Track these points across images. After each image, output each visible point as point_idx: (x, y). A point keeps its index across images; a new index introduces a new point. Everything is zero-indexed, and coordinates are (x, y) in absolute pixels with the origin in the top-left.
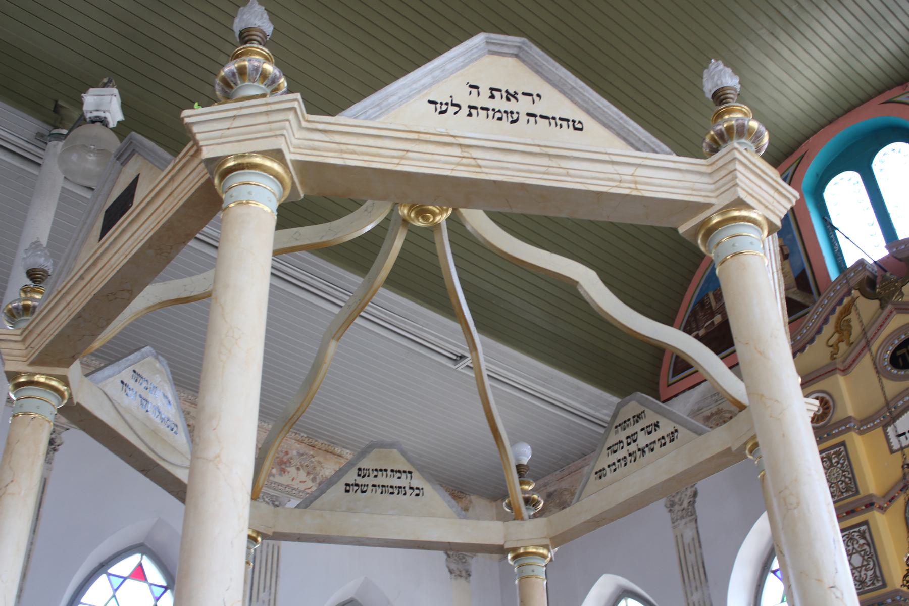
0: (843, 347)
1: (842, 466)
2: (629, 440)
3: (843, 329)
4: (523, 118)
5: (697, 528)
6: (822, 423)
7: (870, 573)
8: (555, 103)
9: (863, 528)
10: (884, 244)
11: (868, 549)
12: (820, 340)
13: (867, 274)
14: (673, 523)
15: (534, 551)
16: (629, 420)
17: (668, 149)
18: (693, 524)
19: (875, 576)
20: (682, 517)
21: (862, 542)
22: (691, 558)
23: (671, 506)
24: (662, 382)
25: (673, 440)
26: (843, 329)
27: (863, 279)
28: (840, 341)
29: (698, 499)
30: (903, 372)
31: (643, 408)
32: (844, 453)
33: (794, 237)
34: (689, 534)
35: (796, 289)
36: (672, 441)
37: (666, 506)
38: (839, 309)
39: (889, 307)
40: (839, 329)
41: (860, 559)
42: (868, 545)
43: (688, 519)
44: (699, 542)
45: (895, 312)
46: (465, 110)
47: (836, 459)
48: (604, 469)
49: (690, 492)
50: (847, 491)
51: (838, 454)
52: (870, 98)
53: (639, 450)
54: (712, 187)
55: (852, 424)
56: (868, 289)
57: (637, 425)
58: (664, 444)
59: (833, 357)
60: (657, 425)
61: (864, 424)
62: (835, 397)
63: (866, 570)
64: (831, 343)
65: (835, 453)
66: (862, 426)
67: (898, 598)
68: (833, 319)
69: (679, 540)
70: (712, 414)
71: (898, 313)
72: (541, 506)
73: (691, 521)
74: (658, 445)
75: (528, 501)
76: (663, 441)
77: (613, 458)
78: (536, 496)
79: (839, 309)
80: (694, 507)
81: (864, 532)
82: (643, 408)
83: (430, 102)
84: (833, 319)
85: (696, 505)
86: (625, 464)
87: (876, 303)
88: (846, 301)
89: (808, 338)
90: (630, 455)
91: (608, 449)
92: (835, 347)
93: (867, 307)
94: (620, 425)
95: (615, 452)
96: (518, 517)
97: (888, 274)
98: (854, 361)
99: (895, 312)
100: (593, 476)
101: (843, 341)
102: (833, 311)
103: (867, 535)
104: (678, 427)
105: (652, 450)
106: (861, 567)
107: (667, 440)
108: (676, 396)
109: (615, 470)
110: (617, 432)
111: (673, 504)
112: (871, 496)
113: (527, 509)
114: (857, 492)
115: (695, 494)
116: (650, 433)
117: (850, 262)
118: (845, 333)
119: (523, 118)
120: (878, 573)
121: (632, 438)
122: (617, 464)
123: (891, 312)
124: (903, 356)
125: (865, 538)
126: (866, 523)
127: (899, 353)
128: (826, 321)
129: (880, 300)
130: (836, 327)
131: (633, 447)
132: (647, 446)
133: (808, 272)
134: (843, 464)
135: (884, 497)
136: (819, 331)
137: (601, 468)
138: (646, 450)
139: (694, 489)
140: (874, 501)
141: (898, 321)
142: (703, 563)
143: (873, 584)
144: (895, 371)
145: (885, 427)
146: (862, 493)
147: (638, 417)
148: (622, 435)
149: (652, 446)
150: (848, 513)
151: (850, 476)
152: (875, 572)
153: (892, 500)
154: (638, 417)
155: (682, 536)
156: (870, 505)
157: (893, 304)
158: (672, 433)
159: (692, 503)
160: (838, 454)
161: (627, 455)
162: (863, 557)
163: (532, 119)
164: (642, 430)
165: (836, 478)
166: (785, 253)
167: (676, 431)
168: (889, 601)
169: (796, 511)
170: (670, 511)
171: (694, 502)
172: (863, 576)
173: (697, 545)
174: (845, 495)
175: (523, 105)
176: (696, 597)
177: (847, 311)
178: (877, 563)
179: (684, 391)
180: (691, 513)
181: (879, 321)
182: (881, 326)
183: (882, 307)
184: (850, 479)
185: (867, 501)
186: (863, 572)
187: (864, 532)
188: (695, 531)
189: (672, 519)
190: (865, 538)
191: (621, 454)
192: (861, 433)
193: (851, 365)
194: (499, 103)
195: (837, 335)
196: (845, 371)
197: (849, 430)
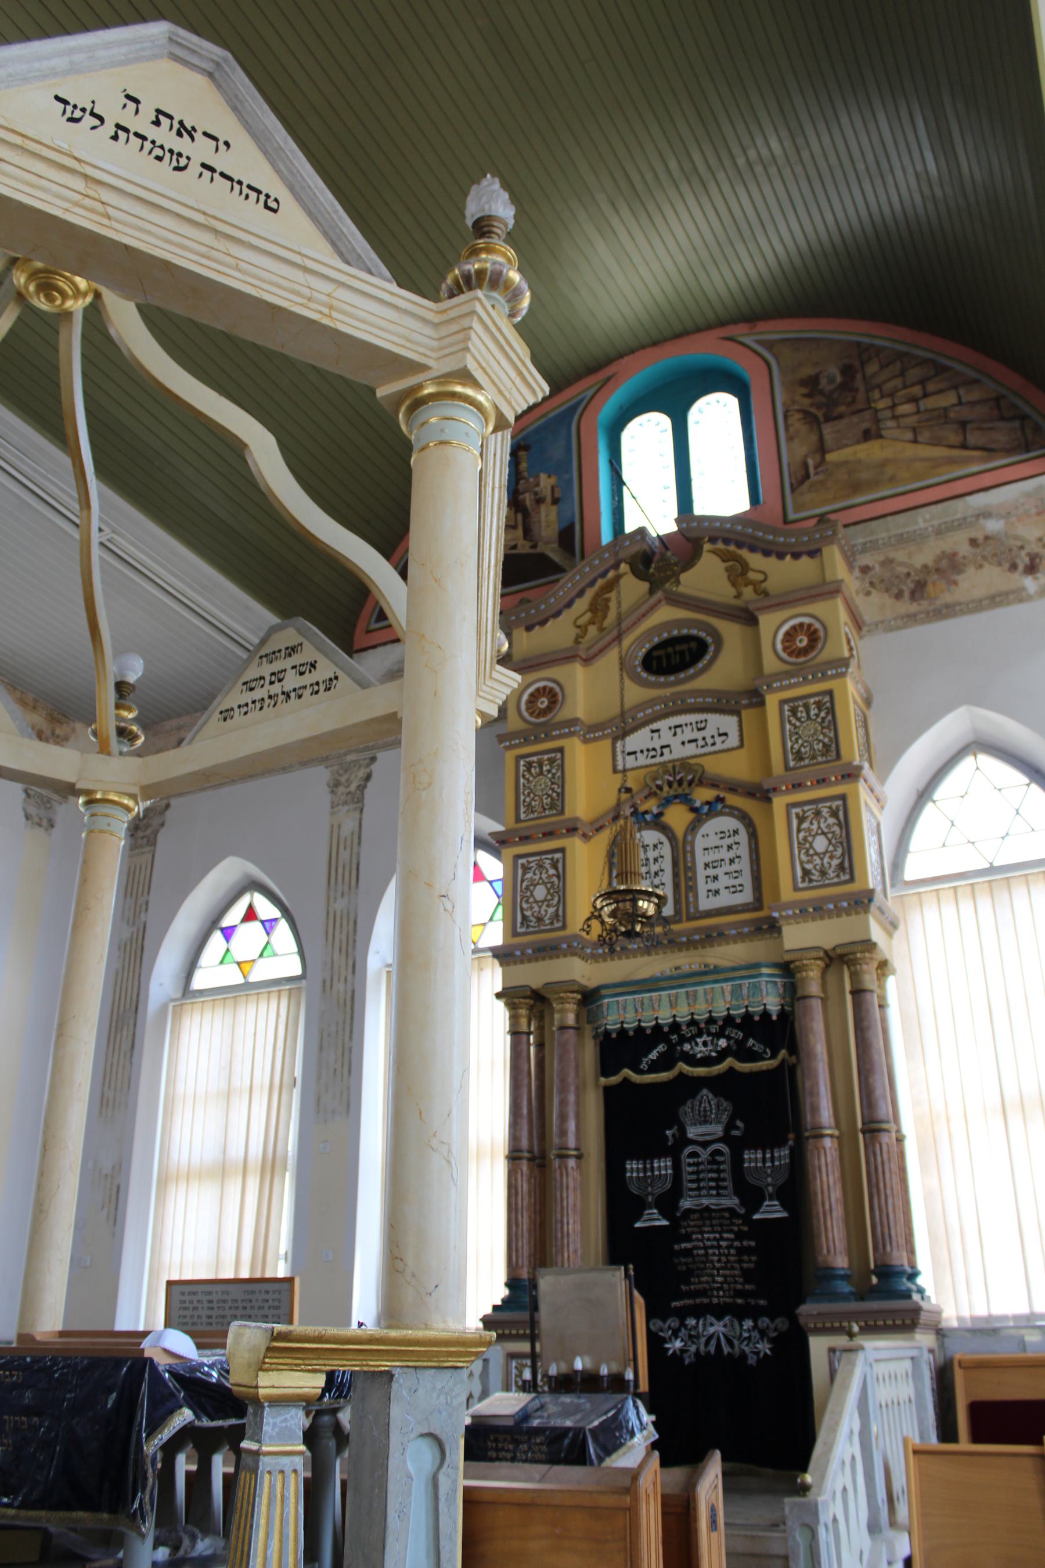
0: (593, 630)
1: (553, 777)
2: (273, 678)
3: (599, 608)
4: (195, 168)
5: (361, 820)
6: (542, 720)
7: (551, 910)
8: (247, 161)
10: (676, 516)
11: (556, 882)
12: (567, 617)
13: (645, 547)
14: (332, 807)
15: (116, 799)
16: (280, 651)
17: (388, 274)
18: (357, 814)
19: (556, 915)
20: (345, 803)
21: (552, 872)
22: (344, 855)
23: (335, 785)
24: (361, 625)
25: (329, 689)
26: (599, 608)
27: (638, 552)
28: (591, 622)
29: (369, 784)
30: (653, 678)
31: (301, 639)
32: (559, 762)
33: (571, 480)
34: (349, 825)
35: (555, 545)
36: (328, 689)
37: (328, 785)
38: (600, 582)
39: (659, 594)
40: (593, 608)
41: (545, 891)
42: (558, 877)
43: (352, 806)
44: (360, 838)
45: (664, 602)
46: (109, 129)
47: (548, 767)
48: (232, 709)
49: (362, 773)
50: (550, 809)
51: (551, 761)
52: (709, 327)
53: (283, 693)
54: (435, 344)
55: (578, 728)
56: (641, 567)
57: (288, 659)
58: (317, 692)
59: (577, 641)
60: (313, 665)
61: (592, 732)
62: (567, 690)
63: (548, 906)
64: (580, 622)
65: (548, 759)
66: (589, 733)
67: (575, 944)
68: (590, 593)
69: (335, 830)
71: (668, 604)
72: (139, 742)
73: (355, 809)
74: (309, 691)
75: (122, 732)
76: (316, 688)
77: (248, 697)
78: (135, 728)
79: (600, 582)
81: (558, 861)
82: (301, 639)
83: (57, 98)
84: (590, 593)
85: (366, 791)
86: (261, 708)
87: (645, 586)
88: (611, 574)
89: (553, 611)
90: (270, 697)
91: (245, 683)
92: (583, 629)
93: (632, 588)
94: (266, 655)
95: (251, 689)
96: (104, 749)
97: (669, 554)
98: (601, 651)
99: (664, 602)
100: (217, 715)
101: (594, 623)
102: (592, 583)
103: (560, 866)
104: (339, 673)
105: (300, 697)
106: (543, 902)
107: (322, 687)
108: (374, 647)
109: (246, 713)
110: (260, 664)
111: (337, 784)
112: (576, 819)
113: (119, 742)
114: (562, 812)
115: (368, 777)
116: (302, 674)
117: (629, 527)
118: (600, 614)
119: (195, 168)
120: (561, 913)
121: (278, 677)
122: (250, 705)
123: (660, 601)
124: (659, 658)
125: (556, 868)
126: (562, 850)
127: (656, 653)
128: (581, 593)
129: (651, 583)
130: (591, 604)
131: (276, 689)
132: (294, 690)
133: (577, 527)
134: (554, 775)
135: (591, 823)
136: (569, 605)
137: (229, 707)
138: (293, 695)
139: (368, 770)
140: (579, 825)
141: (666, 614)
143: (552, 923)
144: (644, 675)
145: (615, 740)
146: (568, 814)
147: (292, 650)
148: (266, 670)
149: (300, 692)
150: (545, 835)
151: (559, 790)
152: (557, 910)
153: (599, 829)
154: (292, 650)
155: (339, 826)
156: (572, 830)
157: (664, 591)
158: (331, 680)
159: (362, 788)
160: (551, 761)
161: (266, 697)
162: (548, 890)
163: (207, 174)
164: (294, 667)
165: (542, 790)
166: (556, 495)
167: (336, 678)
168: (564, 946)
169: (424, 793)
171: (365, 787)
172: (543, 912)
173: (356, 840)
174: (547, 812)
175: (199, 150)
176: (340, 905)
177: (611, 586)
178: (563, 901)
179: (385, 644)
180: (357, 799)
181: (642, 610)
182: (644, 615)
183: (651, 592)
184: (558, 794)
185: (570, 825)
186: (544, 908)
187: (558, 861)
188: (357, 823)
189: (332, 802)
191: (259, 694)
192: (586, 741)
193: (595, 656)
194: (164, 135)
195: (589, 615)
196: (587, 661)
197: (572, 734)
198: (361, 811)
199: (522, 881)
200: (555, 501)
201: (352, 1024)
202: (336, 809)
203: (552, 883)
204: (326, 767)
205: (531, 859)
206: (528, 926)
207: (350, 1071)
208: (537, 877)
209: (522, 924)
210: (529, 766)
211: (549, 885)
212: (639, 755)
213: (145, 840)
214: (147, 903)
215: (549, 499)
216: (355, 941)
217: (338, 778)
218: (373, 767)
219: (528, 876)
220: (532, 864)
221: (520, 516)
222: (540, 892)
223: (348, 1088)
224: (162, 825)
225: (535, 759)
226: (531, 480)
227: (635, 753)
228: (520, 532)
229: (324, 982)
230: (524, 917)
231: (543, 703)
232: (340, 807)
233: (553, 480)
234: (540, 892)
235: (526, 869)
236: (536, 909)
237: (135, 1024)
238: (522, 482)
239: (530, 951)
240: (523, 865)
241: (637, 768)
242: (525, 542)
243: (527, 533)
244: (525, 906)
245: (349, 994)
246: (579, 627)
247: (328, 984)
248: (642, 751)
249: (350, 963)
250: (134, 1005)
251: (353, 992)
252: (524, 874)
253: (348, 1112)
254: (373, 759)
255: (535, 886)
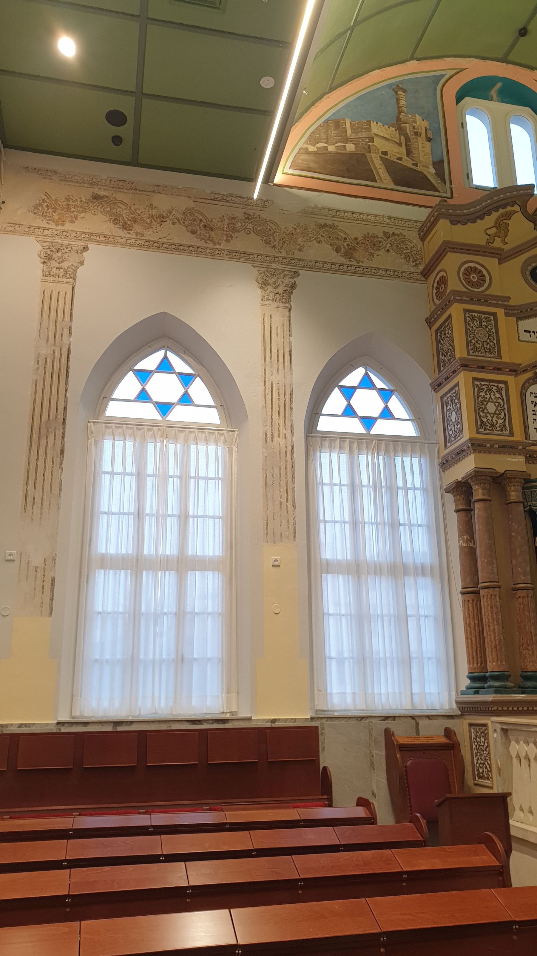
6: (475, 290)
7: (500, 421)
9: (502, 386)
11: (502, 403)
21: (498, 395)
33: (439, 128)
42: (503, 400)
43: (281, 305)
50: (490, 352)
64: (489, 232)
70: (325, 225)
73: (284, 307)
80: (290, 298)
84: (495, 215)
115: (293, 286)
136: (482, 218)
142: (290, 351)
162: (497, 407)
170: (261, 287)
177: (509, 216)
190: (501, 394)
198: (290, 310)
199: (478, 397)
200: (429, 140)
201: (293, 471)
202: (266, 302)
203: (499, 403)
204: (254, 267)
205: (483, 383)
206: (485, 429)
207: (294, 506)
208: (488, 396)
209: (481, 425)
210: (473, 319)
211: (497, 404)
212: (531, 333)
213: (61, 272)
214: (70, 329)
215: (423, 135)
216: (291, 409)
217: (266, 278)
218: (295, 279)
219: (482, 394)
220: (484, 387)
221: (402, 137)
222: (491, 408)
223: (294, 518)
224: (82, 263)
225: (476, 315)
226: (410, 116)
227: (529, 332)
228: (403, 149)
229: (266, 434)
230: (482, 422)
231: (474, 277)
232: (270, 302)
233: (425, 124)
234: (491, 408)
235: (481, 390)
236: (490, 418)
237: (63, 434)
238: (402, 114)
239: (496, 446)
240: (477, 385)
241: (528, 342)
242: (408, 159)
243: (409, 153)
244: (482, 414)
245: (289, 448)
246: (489, 235)
247: (269, 435)
248: (534, 332)
249: (289, 424)
250: (60, 417)
251: (293, 446)
252: (479, 392)
253: (295, 537)
254: (296, 274)
255: (488, 402)
